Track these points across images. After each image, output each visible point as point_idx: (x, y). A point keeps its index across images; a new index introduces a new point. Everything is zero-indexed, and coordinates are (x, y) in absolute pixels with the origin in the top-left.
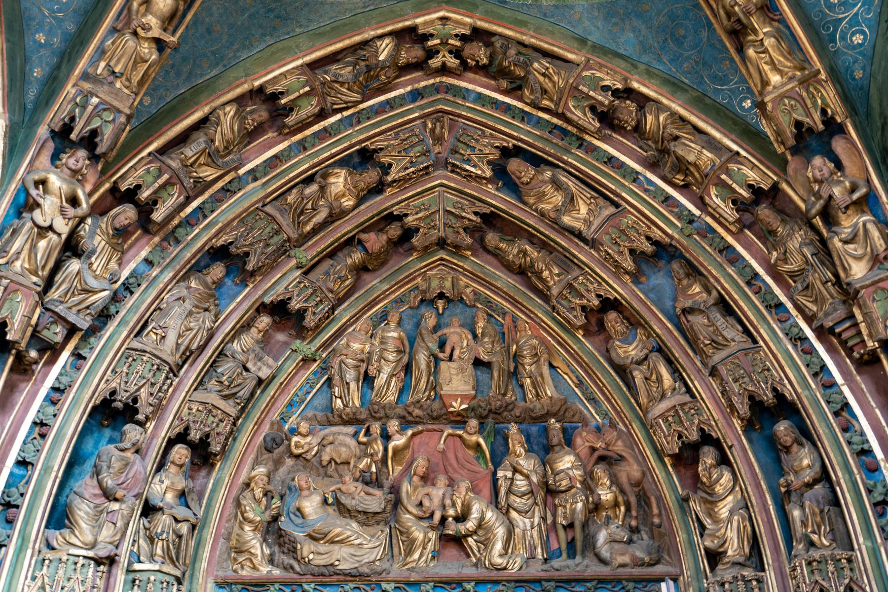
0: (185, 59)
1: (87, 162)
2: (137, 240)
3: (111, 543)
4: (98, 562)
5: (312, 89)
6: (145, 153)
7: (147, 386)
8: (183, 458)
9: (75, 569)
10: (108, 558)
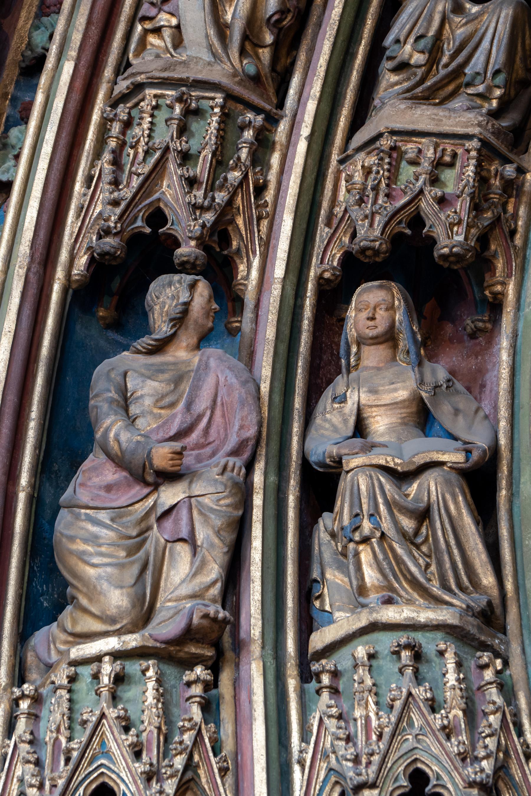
3: (193, 596)
4: (172, 654)
7: (171, 166)
8: (381, 314)
9: (98, 694)
10: (189, 634)
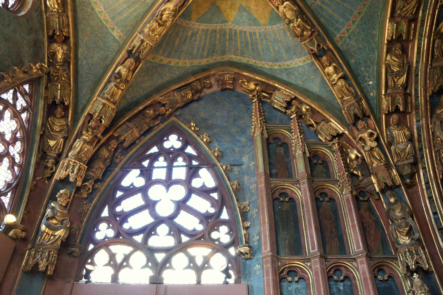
0: (365, 62)
1: (364, 122)
2: (410, 118)
5: (397, 23)
6: (383, 96)
